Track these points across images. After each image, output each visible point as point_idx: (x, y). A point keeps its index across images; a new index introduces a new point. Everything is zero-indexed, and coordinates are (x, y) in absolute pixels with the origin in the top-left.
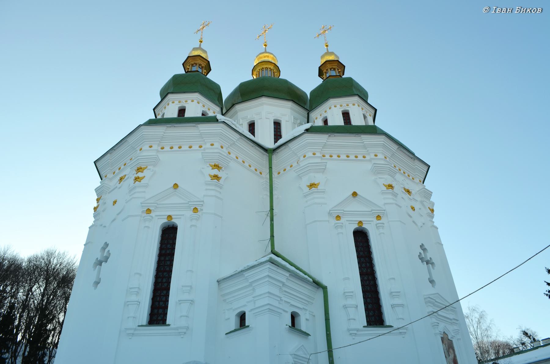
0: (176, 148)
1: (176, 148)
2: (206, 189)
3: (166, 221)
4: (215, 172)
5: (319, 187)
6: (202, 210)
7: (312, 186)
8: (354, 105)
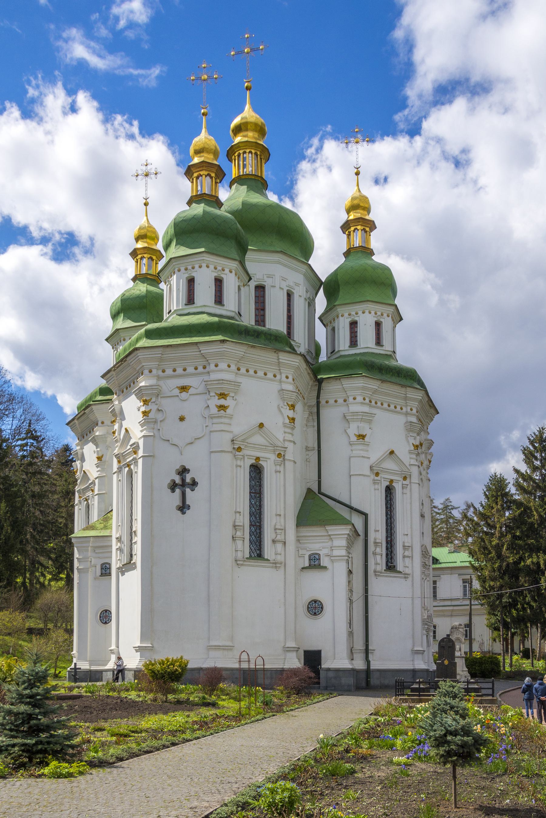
0: (251, 372)
1: (251, 372)
2: (285, 432)
3: (254, 461)
4: (291, 414)
5: (366, 439)
6: (284, 455)
7: (362, 437)
8: (388, 316)
